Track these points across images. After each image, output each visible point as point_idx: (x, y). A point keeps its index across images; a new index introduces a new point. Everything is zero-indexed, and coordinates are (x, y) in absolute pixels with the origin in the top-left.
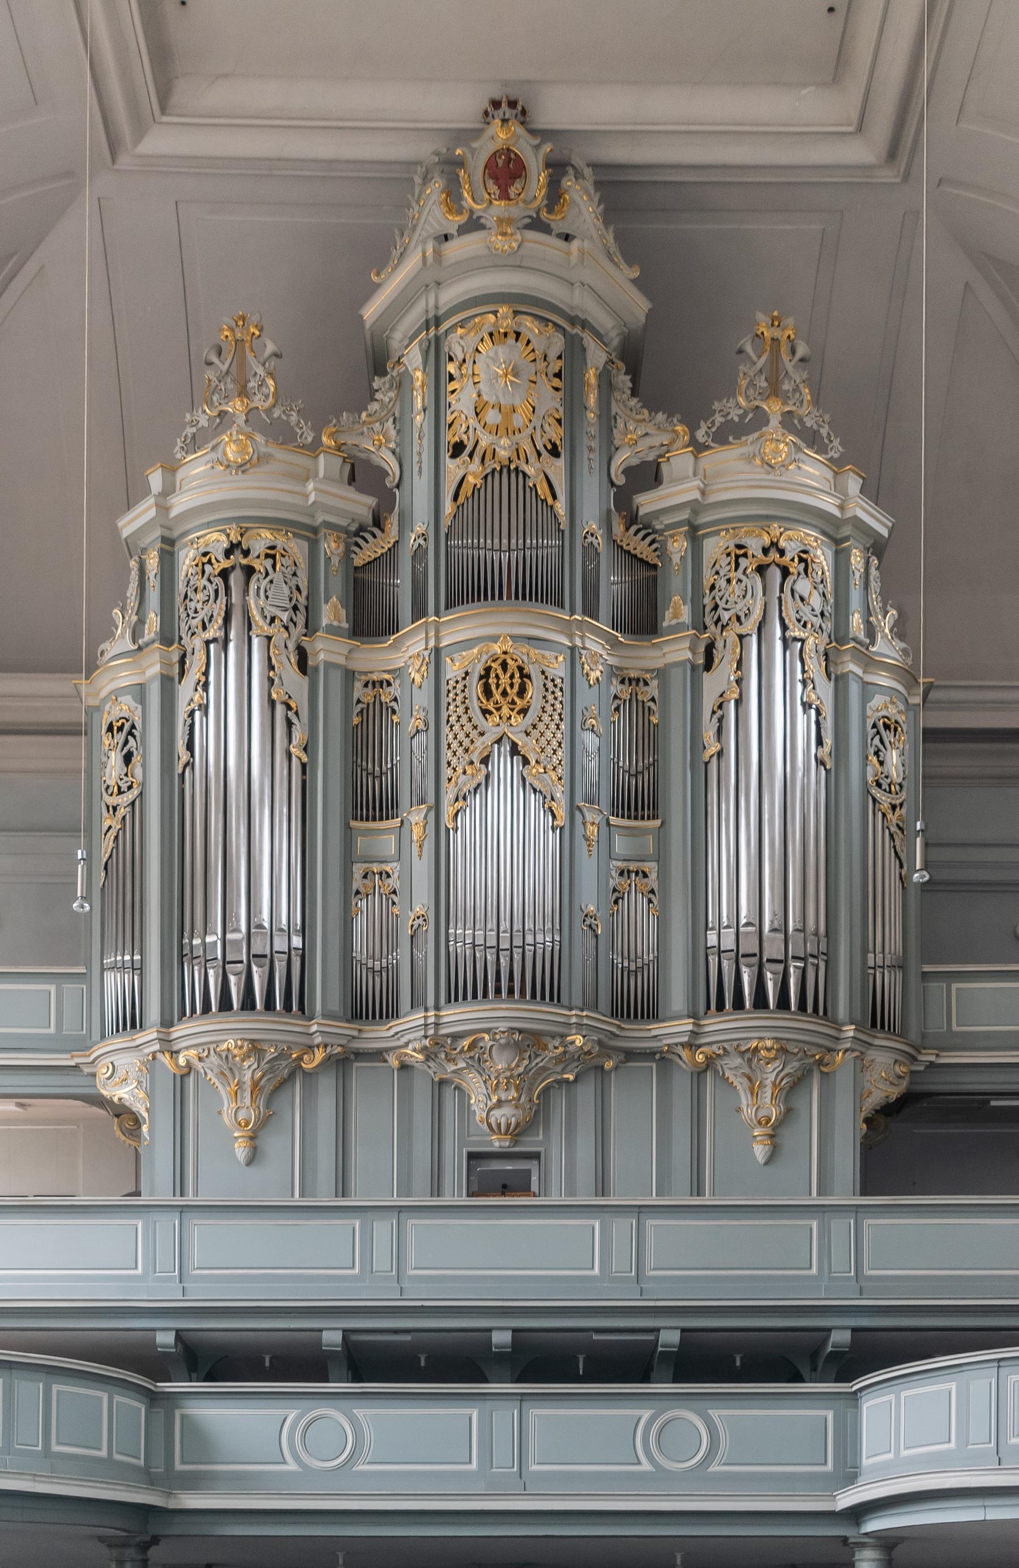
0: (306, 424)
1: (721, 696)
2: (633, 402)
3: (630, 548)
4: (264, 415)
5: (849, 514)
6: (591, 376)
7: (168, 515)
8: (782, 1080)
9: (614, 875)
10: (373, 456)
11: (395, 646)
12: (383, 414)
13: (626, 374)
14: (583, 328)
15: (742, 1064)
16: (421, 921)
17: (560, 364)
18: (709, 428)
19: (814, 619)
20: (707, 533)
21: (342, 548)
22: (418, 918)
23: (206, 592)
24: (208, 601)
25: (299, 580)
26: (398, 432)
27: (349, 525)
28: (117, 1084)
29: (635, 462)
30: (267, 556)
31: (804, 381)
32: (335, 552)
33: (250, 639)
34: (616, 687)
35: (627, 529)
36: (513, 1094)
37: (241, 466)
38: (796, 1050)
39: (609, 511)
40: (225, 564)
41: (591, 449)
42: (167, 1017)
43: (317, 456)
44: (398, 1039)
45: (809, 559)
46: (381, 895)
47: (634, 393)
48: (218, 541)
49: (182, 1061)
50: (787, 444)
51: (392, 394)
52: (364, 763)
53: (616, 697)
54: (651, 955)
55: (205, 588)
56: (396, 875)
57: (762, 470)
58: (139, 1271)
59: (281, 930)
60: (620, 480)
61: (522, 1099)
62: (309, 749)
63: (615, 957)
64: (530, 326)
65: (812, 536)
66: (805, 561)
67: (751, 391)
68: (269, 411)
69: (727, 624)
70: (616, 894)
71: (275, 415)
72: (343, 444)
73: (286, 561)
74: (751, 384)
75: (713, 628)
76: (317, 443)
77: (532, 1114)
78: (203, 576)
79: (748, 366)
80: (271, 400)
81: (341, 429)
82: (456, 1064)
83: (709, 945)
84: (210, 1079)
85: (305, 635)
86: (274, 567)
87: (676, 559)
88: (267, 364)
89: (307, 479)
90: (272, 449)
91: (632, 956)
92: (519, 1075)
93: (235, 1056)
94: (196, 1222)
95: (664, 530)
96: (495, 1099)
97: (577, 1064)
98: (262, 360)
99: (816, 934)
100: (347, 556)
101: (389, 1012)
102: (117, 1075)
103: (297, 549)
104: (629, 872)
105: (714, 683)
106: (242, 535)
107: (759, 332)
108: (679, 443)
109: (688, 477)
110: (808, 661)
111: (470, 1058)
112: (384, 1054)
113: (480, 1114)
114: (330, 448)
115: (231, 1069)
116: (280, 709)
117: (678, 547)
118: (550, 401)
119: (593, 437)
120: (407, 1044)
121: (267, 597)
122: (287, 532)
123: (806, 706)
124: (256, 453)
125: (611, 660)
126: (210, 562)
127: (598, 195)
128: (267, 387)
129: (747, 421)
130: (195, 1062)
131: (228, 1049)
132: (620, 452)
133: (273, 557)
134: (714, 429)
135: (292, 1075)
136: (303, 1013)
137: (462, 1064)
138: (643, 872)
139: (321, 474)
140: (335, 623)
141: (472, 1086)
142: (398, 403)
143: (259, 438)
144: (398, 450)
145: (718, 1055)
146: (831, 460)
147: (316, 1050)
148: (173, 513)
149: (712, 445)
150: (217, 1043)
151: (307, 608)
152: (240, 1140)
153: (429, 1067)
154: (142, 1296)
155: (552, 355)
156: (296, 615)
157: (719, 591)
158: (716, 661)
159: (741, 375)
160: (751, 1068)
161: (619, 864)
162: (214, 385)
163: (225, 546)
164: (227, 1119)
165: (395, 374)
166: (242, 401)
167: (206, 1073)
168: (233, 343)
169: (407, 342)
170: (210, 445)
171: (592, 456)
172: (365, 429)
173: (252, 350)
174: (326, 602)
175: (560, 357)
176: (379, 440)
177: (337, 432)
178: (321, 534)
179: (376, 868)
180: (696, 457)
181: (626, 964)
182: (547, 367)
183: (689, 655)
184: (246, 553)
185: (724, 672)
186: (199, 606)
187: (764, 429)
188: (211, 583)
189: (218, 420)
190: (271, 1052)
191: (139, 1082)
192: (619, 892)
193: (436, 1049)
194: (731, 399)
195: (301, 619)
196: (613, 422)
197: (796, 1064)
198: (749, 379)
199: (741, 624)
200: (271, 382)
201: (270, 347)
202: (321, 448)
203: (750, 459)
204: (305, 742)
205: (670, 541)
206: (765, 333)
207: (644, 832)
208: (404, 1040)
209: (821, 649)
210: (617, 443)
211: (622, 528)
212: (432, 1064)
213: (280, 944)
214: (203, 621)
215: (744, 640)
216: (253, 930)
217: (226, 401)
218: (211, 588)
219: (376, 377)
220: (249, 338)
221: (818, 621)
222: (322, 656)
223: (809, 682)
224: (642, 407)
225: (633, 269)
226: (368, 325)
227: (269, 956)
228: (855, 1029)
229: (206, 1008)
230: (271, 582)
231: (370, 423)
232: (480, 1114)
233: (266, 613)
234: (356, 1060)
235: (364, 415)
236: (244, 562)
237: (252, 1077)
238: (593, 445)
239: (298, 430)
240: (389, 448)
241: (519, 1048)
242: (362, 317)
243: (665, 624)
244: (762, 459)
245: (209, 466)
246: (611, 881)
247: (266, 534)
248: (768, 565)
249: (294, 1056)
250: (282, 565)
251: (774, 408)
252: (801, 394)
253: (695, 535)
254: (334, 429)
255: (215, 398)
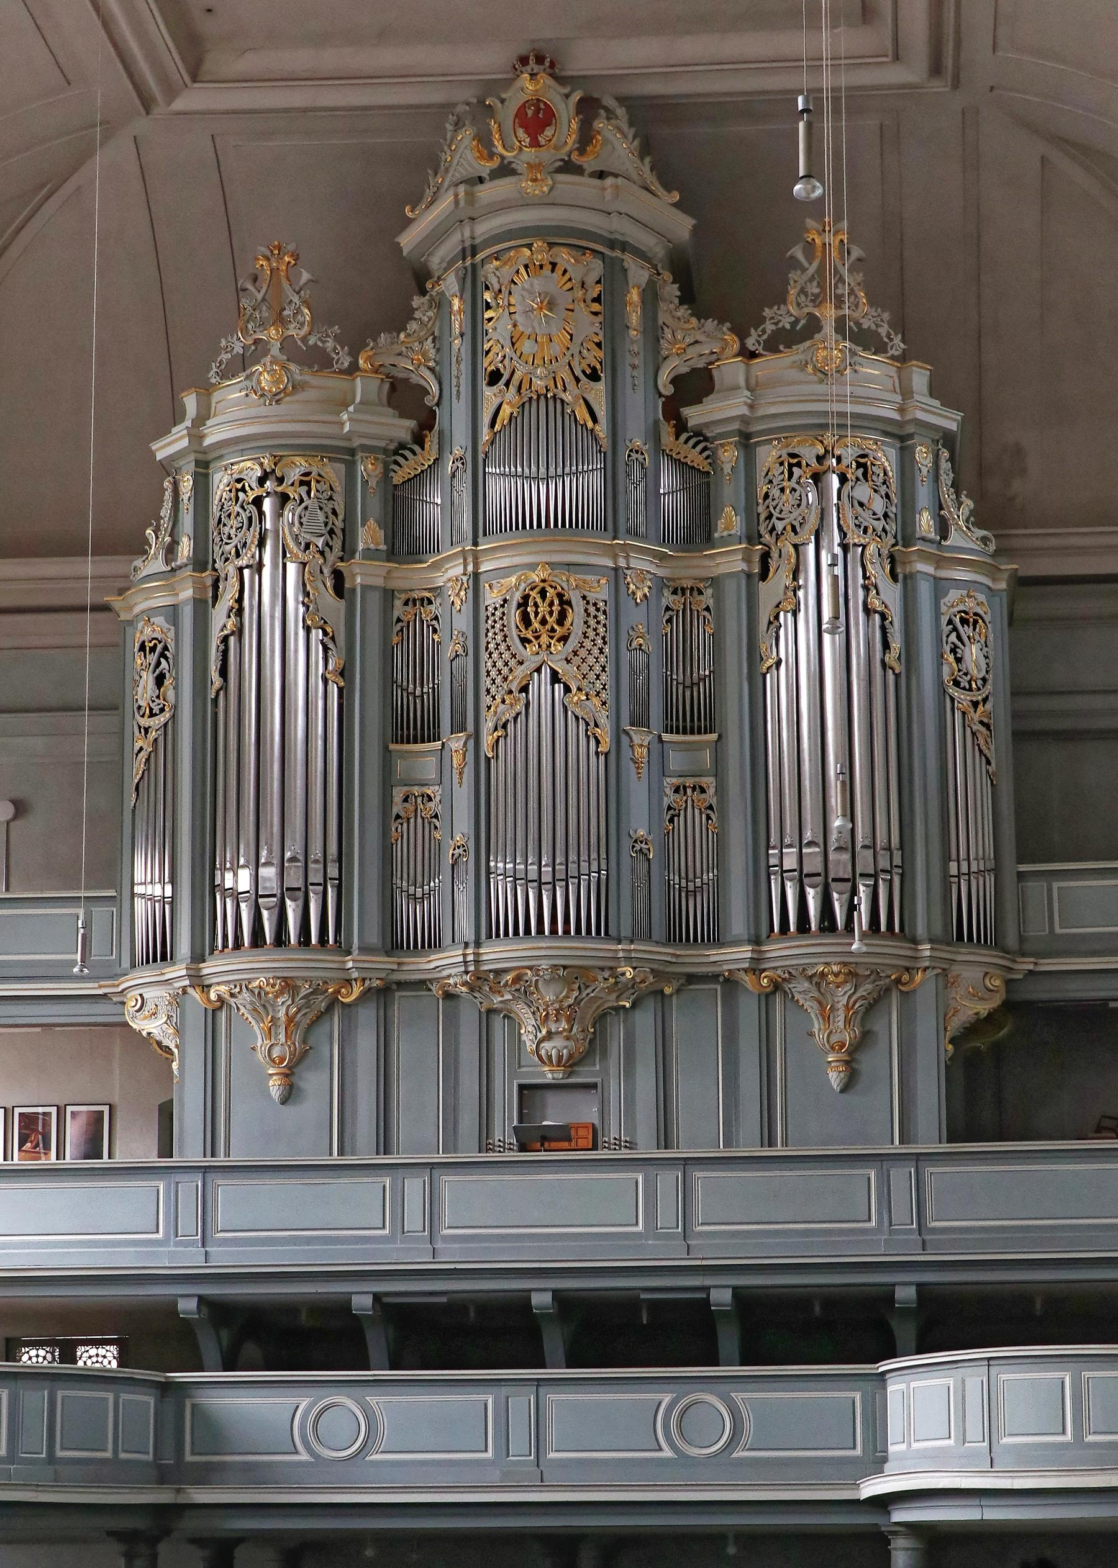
0: (343, 348)
1: (778, 606)
2: (683, 311)
3: (681, 457)
4: (299, 342)
5: (908, 417)
6: (634, 296)
7: (201, 444)
8: (855, 1002)
9: (668, 793)
10: (413, 375)
11: (436, 566)
12: (422, 334)
13: (674, 282)
14: (623, 251)
15: (810, 988)
16: (461, 851)
17: (598, 288)
18: (759, 336)
19: (875, 523)
20: (758, 442)
21: (380, 468)
22: (459, 847)
23: (239, 519)
24: (242, 527)
25: (336, 503)
26: (438, 350)
27: (387, 445)
28: (145, 1018)
29: (684, 369)
30: (302, 483)
31: (859, 284)
32: (370, 473)
33: (284, 566)
34: (668, 598)
35: (677, 439)
36: (564, 1025)
37: (276, 395)
38: (869, 973)
39: (656, 422)
40: (258, 491)
41: (634, 367)
42: (199, 951)
43: (354, 379)
44: (440, 971)
45: (869, 463)
46: (423, 818)
47: (683, 300)
48: (252, 469)
49: (213, 996)
50: (840, 350)
51: (430, 313)
52: (405, 684)
53: (668, 609)
54: (711, 875)
55: (238, 514)
56: (438, 798)
57: (815, 378)
58: (160, 1235)
59: (316, 861)
60: (668, 390)
61: (574, 1030)
62: (346, 673)
63: (671, 878)
64: (564, 257)
65: (871, 439)
66: (864, 466)
67: (803, 298)
68: (304, 339)
69: (782, 534)
70: (672, 812)
71: (311, 342)
72: (381, 365)
73: (323, 487)
74: (803, 291)
75: (767, 538)
76: (354, 368)
77: (587, 1045)
78: (237, 502)
79: (799, 272)
80: (306, 328)
81: (378, 351)
82: (502, 996)
83: (771, 863)
84: (243, 1014)
85: (342, 559)
86: (309, 493)
87: (727, 469)
88: (302, 292)
89: (345, 405)
90: (307, 378)
91: (691, 876)
92: (570, 1006)
93: (268, 993)
94: (220, 1182)
95: (715, 438)
96: (544, 1031)
97: (633, 991)
98: (297, 289)
99: (889, 848)
100: (386, 476)
101: (433, 943)
102: (146, 1008)
103: (333, 473)
104: (685, 788)
105: (771, 591)
106: (275, 464)
107: (809, 240)
108: (729, 352)
109: (738, 388)
110: (869, 566)
111: (516, 990)
112: (428, 983)
113: (530, 1045)
114: (366, 371)
115: (264, 1006)
116: (317, 635)
117: (729, 456)
118: (588, 326)
119: (637, 354)
120: (449, 976)
121: (301, 524)
122: (322, 457)
123: (868, 611)
124: (291, 380)
125: (660, 572)
126: (243, 490)
127: (633, 131)
128: (303, 315)
129: (798, 328)
130: (227, 996)
131: (260, 987)
132: (668, 361)
133: (308, 484)
134: (765, 337)
135: (330, 1008)
136: (340, 947)
137: (508, 997)
138: (700, 787)
139: (358, 400)
140: (372, 546)
141: (521, 1015)
142: (438, 324)
143: (293, 367)
144: (437, 368)
145: (784, 980)
146: (893, 358)
147: (354, 983)
148: (207, 442)
149: (764, 353)
150: (250, 981)
151: (343, 530)
152: (275, 1078)
153: (475, 997)
154: (162, 1261)
155: (591, 280)
156: (332, 539)
157: (773, 500)
158: (772, 570)
159: (792, 283)
160: (819, 991)
161: (674, 780)
162: (249, 313)
163: (259, 475)
164: (260, 1056)
165: (434, 293)
166: (277, 330)
167: (238, 1008)
168: (268, 272)
169: (444, 265)
170: (244, 374)
171: (635, 373)
172: (404, 349)
173: (288, 279)
174: (363, 525)
175: (599, 282)
176: (419, 359)
177: (375, 354)
178: (358, 457)
179: (416, 790)
180: (748, 365)
181: (684, 884)
182: (585, 294)
183: (743, 566)
184: (280, 480)
185: (780, 578)
186: (233, 532)
187: (817, 336)
188: (245, 510)
189: (253, 348)
190: (305, 989)
191: (169, 1017)
192: (675, 810)
193: (479, 983)
194: (782, 306)
195: (337, 543)
196: (660, 331)
197: (870, 987)
198: (799, 287)
199: (796, 533)
200: (306, 311)
201: (305, 276)
202: (358, 373)
203: (803, 366)
204: (341, 666)
205: (720, 452)
206: (816, 241)
207: (699, 747)
208: (445, 973)
209: (885, 552)
210: (665, 353)
211: (672, 439)
212: (477, 995)
213: (316, 877)
214: (236, 547)
215: (801, 548)
216: (286, 864)
217: (261, 329)
218: (244, 516)
219: (415, 297)
220: (284, 268)
221: (879, 525)
222: (359, 580)
223: (872, 588)
224: (692, 315)
225: (672, 195)
226: (405, 254)
227: (303, 889)
228: (931, 949)
229: (238, 945)
230: (306, 508)
231: (409, 343)
232: (530, 1045)
233: (301, 539)
234: (398, 990)
235: (402, 336)
236: (279, 489)
237: (287, 1014)
238: (636, 362)
239: (334, 356)
240: (429, 368)
241: (568, 982)
242: (399, 244)
243: (716, 535)
244: (815, 367)
245: (243, 393)
246: (665, 799)
247: (299, 460)
248: (825, 472)
249: (330, 990)
250: (318, 491)
251: (828, 314)
252: (856, 296)
253: (746, 441)
254: (370, 353)
255: (250, 326)
